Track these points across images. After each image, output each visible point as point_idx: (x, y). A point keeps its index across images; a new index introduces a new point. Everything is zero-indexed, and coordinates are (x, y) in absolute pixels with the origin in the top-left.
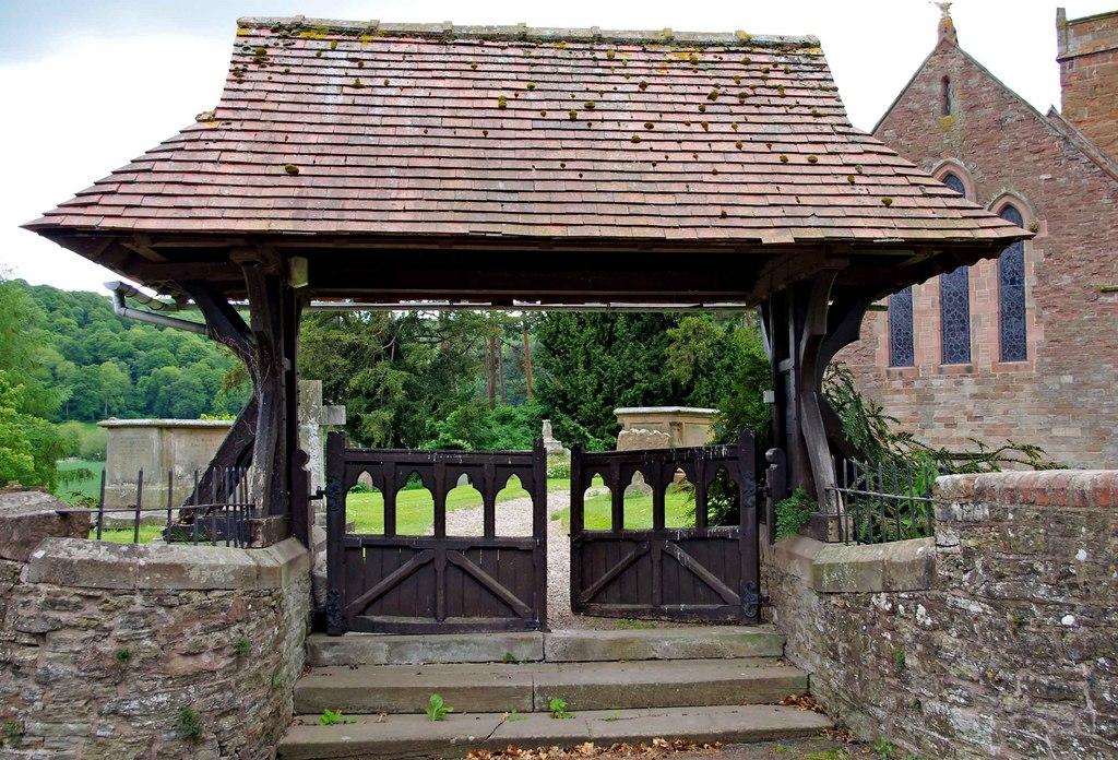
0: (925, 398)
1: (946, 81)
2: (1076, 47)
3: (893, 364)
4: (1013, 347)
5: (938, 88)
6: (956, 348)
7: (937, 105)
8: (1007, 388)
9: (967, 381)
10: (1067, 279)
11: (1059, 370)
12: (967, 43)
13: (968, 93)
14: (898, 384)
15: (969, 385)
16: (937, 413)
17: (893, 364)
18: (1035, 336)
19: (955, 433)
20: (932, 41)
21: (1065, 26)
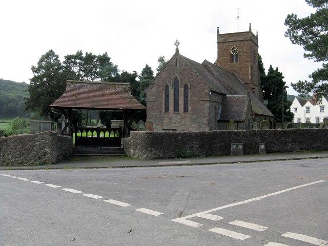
0: (171, 119)
1: (176, 60)
2: (221, 40)
3: (165, 112)
4: (186, 110)
5: (175, 61)
6: (176, 110)
7: (175, 64)
8: (185, 118)
9: (178, 116)
10: (195, 98)
11: (193, 114)
12: (181, 53)
13: (180, 63)
14: (166, 116)
15: (179, 117)
16: (173, 121)
17: (165, 112)
18: (190, 108)
19: (176, 125)
20: (174, 52)
21: (219, 35)
